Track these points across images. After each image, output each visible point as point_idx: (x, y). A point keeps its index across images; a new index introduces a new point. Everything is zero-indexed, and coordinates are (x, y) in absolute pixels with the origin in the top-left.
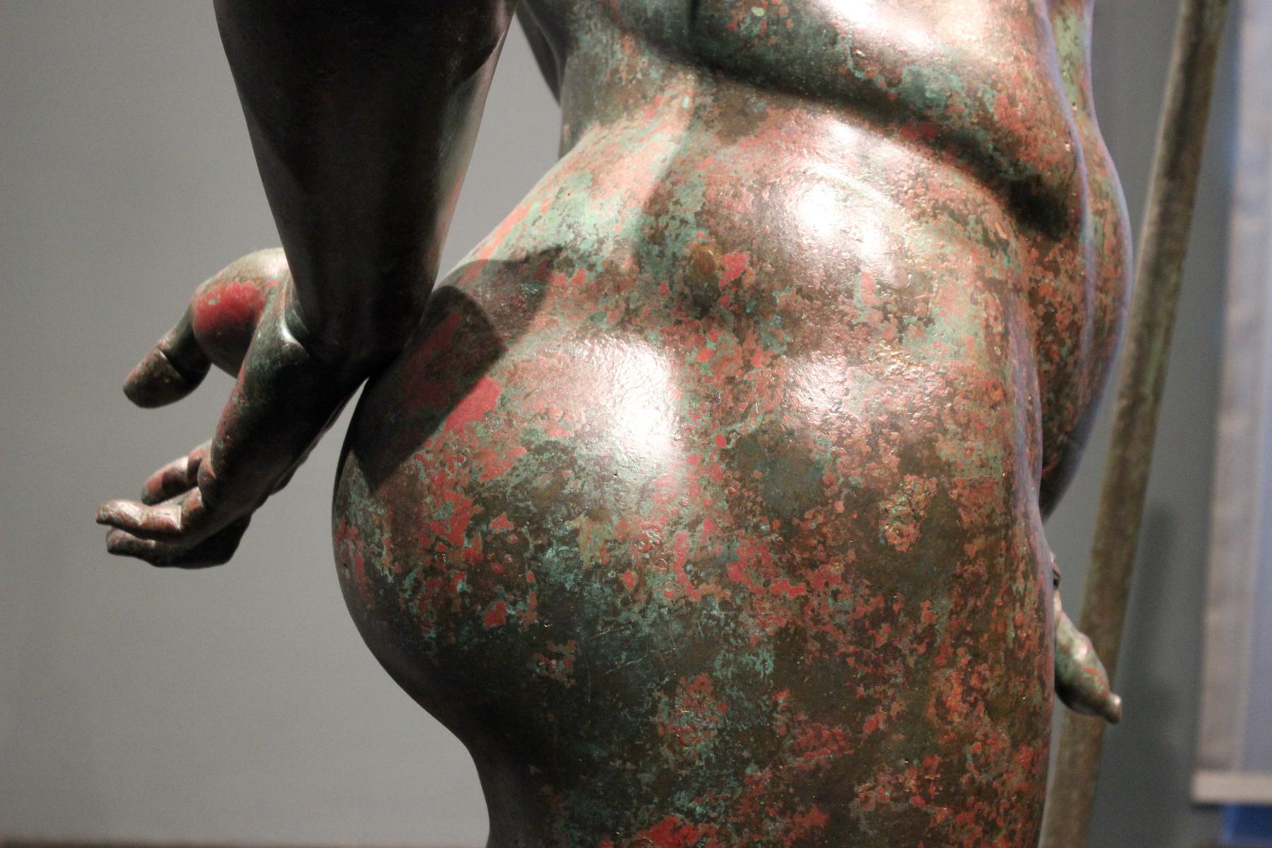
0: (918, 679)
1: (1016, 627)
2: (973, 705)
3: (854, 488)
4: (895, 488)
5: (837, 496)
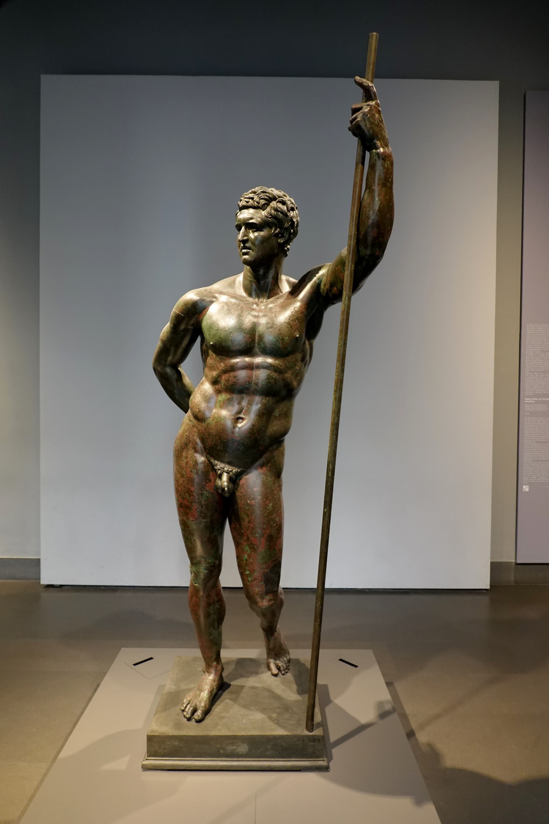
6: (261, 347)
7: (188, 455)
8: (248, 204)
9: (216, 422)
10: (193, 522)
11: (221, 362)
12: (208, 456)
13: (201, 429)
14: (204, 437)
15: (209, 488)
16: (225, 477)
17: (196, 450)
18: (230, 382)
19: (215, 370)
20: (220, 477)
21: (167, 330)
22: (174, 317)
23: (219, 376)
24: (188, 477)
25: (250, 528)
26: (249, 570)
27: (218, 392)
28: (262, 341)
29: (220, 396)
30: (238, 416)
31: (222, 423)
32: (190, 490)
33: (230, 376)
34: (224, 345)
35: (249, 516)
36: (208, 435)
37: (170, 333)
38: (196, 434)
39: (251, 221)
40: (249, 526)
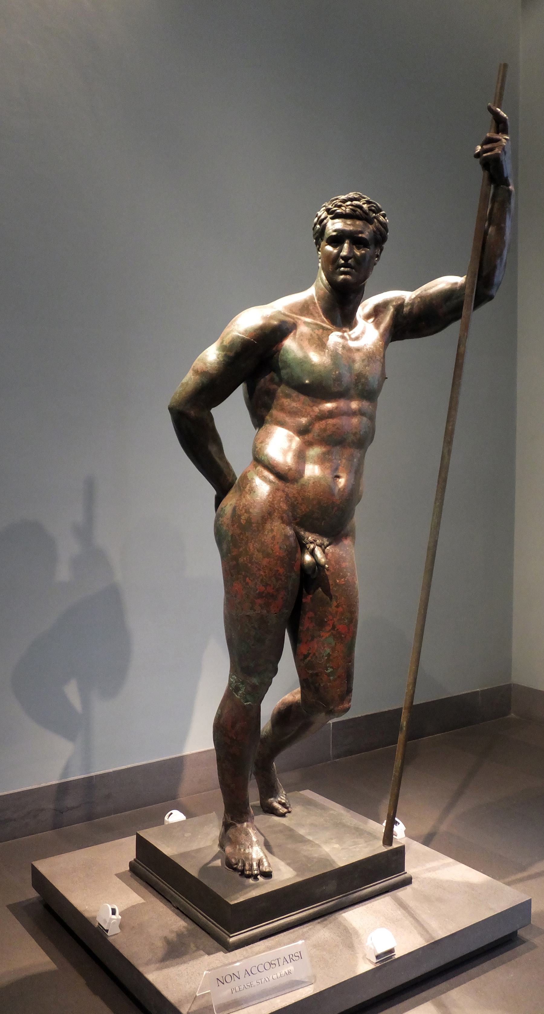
0: (247, 543)
1: (264, 539)
2: (255, 549)
3: (238, 514)
4: (243, 515)
5: (236, 516)
6: (358, 389)
7: (274, 527)
8: (355, 214)
9: (313, 483)
10: (276, 615)
11: (314, 405)
12: (297, 527)
13: (292, 492)
14: (296, 503)
15: (297, 569)
17: (284, 520)
18: (328, 432)
19: (303, 416)
21: (217, 359)
22: (240, 343)
23: (311, 424)
24: (277, 556)
25: (338, 613)
26: (332, 667)
28: (360, 381)
29: (311, 449)
30: (335, 474)
31: (322, 483)
32: (279, 572)
33: (327, 424)
34: (324, 385)
35: (338, 598)
36: (302, 499)
37: (224, 364)
38: (282, 499)
39: (360, 235)
40: (337, 612)
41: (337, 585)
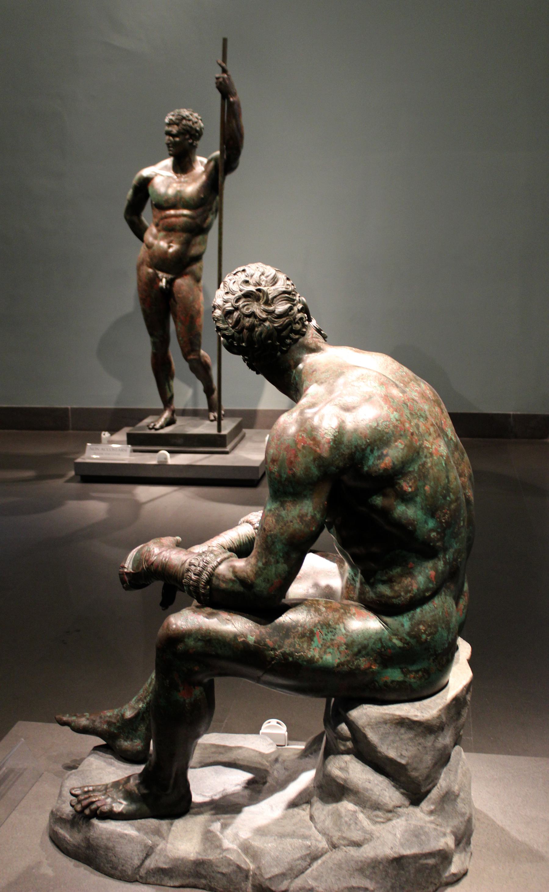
16: (164, 280)
20: (161, 280)
23: (159, 221)
27: (159, 231)
41: (179, 297)
